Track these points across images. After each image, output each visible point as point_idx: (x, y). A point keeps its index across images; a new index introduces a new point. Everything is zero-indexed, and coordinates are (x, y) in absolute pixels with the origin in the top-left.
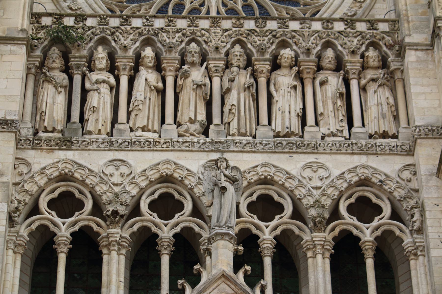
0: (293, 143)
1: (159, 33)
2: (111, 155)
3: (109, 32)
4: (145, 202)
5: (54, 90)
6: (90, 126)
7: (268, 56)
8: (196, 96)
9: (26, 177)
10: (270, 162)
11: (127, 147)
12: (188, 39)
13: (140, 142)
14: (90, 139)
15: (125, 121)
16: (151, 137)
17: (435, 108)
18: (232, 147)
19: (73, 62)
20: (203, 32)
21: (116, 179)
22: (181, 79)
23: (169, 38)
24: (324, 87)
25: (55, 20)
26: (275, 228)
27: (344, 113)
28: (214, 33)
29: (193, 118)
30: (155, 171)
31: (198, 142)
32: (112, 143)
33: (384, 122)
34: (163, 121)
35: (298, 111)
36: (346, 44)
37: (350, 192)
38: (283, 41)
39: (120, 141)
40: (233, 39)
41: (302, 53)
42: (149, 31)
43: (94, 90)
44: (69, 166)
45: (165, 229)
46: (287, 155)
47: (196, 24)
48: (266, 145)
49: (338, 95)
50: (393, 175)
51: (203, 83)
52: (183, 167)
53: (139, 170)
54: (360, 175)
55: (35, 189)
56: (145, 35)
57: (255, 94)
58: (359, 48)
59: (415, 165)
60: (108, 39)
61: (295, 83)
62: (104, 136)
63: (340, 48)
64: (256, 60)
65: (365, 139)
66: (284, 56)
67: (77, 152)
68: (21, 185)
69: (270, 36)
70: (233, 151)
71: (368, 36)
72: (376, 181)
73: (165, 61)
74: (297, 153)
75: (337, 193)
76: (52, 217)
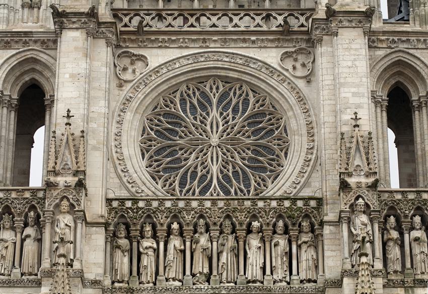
1: (181, 211)
3: (152, 211)
5: (122, 254)
6: (143, 279)
7: (244, 227)
12: (198, 215)
13: (171, 289)
14: (144, 288)
17: (338, 267)
19: (133, 233)
20: (207, 210)
22: (194, 243)
24: (276, 248)
25: (120, 204)
27: (287, 265)
28: (213, 210)
29: (201, 271)
31: (204, 288)
35: (261, 265)
38: (254, 215)
39: (160, 288)
40: (224, 215)
41: (265, 224)
42: (175, 210)
43: (145, 254)
47: (203, 204)
48: (242, 289)
58: (298, 220)
60: (151, 216)
61: (260, 245)
62: (151, 285)
64: (238, 230)
71: (304, 211)
73: (185, 232)
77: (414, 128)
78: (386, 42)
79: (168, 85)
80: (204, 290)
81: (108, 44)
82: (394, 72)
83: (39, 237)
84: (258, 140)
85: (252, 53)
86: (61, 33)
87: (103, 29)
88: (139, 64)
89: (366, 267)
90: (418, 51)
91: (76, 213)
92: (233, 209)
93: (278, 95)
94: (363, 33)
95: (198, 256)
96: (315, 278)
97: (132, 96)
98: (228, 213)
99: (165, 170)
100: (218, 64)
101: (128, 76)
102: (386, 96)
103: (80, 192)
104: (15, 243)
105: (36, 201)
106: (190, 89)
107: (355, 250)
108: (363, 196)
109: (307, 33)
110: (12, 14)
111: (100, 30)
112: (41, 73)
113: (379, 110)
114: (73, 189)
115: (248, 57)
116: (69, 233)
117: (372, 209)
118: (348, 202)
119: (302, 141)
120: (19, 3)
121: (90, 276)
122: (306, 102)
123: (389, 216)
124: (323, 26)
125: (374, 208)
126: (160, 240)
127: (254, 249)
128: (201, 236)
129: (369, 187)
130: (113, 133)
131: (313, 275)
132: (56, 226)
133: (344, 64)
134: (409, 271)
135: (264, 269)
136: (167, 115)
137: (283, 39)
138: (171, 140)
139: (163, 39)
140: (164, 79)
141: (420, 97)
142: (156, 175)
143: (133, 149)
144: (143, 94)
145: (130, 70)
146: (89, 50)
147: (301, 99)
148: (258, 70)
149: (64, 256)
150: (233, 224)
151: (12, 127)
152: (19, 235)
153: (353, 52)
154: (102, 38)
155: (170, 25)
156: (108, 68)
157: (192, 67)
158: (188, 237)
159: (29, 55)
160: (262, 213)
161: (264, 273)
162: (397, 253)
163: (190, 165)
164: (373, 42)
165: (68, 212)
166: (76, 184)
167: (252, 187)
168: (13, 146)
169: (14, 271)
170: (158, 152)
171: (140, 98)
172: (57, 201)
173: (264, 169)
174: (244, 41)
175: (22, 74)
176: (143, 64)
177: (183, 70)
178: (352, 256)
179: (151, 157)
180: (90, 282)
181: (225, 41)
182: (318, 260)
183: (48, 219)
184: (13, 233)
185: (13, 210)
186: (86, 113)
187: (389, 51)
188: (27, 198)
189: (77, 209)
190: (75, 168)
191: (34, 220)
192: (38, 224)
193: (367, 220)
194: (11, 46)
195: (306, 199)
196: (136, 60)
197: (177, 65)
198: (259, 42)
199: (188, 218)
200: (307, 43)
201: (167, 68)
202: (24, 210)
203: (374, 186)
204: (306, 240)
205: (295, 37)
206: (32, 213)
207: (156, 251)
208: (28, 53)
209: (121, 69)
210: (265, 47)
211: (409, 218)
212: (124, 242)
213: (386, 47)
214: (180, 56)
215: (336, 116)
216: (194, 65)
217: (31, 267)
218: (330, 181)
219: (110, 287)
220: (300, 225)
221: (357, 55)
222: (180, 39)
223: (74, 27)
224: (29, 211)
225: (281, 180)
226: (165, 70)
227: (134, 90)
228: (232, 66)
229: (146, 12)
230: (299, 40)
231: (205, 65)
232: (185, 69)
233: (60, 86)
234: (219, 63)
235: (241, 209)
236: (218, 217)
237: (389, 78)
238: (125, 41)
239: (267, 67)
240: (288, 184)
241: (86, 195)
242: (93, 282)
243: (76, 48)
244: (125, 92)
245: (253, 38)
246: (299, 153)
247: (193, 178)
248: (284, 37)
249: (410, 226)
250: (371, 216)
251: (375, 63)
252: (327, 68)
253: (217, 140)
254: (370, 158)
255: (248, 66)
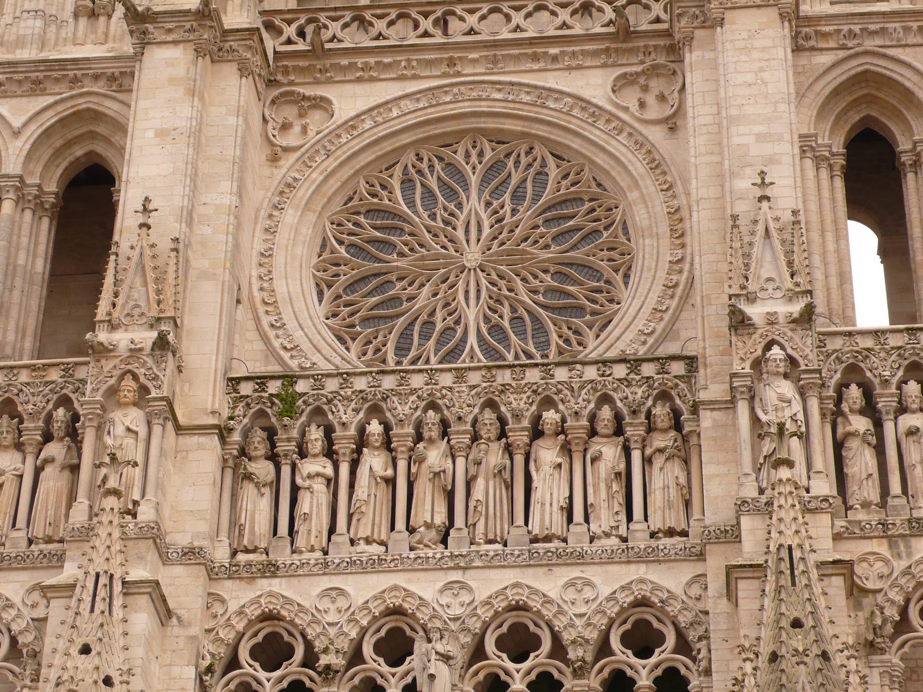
0: (552, 552)
2: (327, 582)
4: (368, 642)
5: (256, 491)
6: (300, 542)
7: (526, 423)
8: (434, 486)
9: (222, 621)
10: (523, 581)
11: (346, 568)
14: (300, 561)
15: (345, 530)
16: (375, 553)
18: (477, 560)
21: (330, 618)
22: (415, 463)
23: (400, 404)
24: (596, 465)
26: (528, 673)
27: (621, 501)
28: (459, 392)
29: (429, 521)
30: (380, 601)
31: (434, 557)
32: (326, 565)
33: (670, 514)
34: (393, 528)
36: (626, 398)
37: (624, 616)
39: (337, 561)
40: (482, 400)
44: (274, 600)
45: (393, 681)
46: (546, 569)
48: (519, 556)
49: (613, 476)
50: (678, 591)
51: (442, 468)
52: (414, 594)
53: (361, 601)
54: (636, 593)
55: (231, 636)
56: (371, 400)
57: (509, 480)
58: (644, 404)
59: (705, 575)
61: (559, 460)
62: (318, 554)
63: (619, 404)
65: (646, 540)
66: (547, 421)
67: (284, 580)
68: (214, 632)
69: (529, 393)
70: (478, 567)
71: (656, 384)
72: (657, 601)
73: (395, 439)
74: (558, 565)
75: (605, 621)
76: (254, 672)
77: (906, 209)
78: (835, 37)
79: (375, 152)
80: (435, 561)
81: (244, 70)
82: (855, 96)
83: (75, 461)
84: (567, 251)
85: (553, 80)
86: (143, 54)
87: (232, 43)
88: (315, 119)
89: (789, 488)
90: (908, 50)
91: (151, 404)
92: (500, 388)
93: (608, 159)
94: (778, 16)
95: (424, 489)
96: (683, 526)
97: (298, 176)
98: (491, 396)
99: (366, 320)
100: (480, 106)
101: (291, 139)
102: (841, 146)
103: (163, 361)
104: (21, 477)
105: (71, 387)
106: (422, 159)
107: (765, 457)
108: (782, 341)
109: (668, 34)
110: (53, 28)
111: (227, 45)
112: (107, 140)
113: (824, 174)
114: (147, 356)
115: (544, 88)
116: (133, 447)
117: (803, 367)
118: (748, 355)
119: (658, 249)
120: (70, 7)
121: (180, 538)
122: (666, 169)
123: (847, 386)
124: (693, 9)
125: (807, 365)
126: (341, 459)
127: (547, 469)
128: (431, 447)
129: (794, 321)
130: (254, 251)
131: (678, 520)
132: (106, 433)
133: (740, 78)
134: (897, 501)
135: (569, 511)
136: (371, 212)
137: (617, 50)
138: (380, 261)
139: (366, 63)
140: (368, 141)
141: (915, 144)
142: (346, 332)
143: (298, 282)
144: (321, 173)
145: (297, 129)
146: (198, 82)
147: (656, 166)
148: (564, 113)
149: (116, 493)
150: (502, 421)
151: (42, 248)
152: (30, 460)
153: (756, 55)
154: (230, 61)
155: (379, 36)
156: (240, 118)
157: (426, 115)
158: (403, 449)
159: (82, 103)
160: (566, 392)
161: (570, 520)
162: (867, 464)
163: (420, 308)
164: (807, 38)
165: (135, 404)
166: (154, 343)
167: (553, 348)
168: (42, 287)
169: (15, 534)
170: (351, 287)
171: (315, 180)
172: (112, 381)
173: (579, 310)
174: (535, 58)
175: (69, 144)
176: (325, 115)
177: (406, 121)
178: (760, 469)
179: (339, 297)
180: (179, 550)
181: (495, 60)
182: (690, 488)
183: (90, 419)
184: (18, 456)
185: (20, 408)
186: (186, 203)
187: (842, 54)
188: (53, 382)
189: (153, 395)
190: (154, 313)
191: (64, 425)
192: (73, 435)
193: (792, 392)
194: (45, 89)
195: (662, 359)
196: (309, 107)
197: (395, 112)
198: (566, 58)
199: (403, 410)
200: (668, 54)
201: (373, 118)
202: (44, 407)
203: (807, 317)
204: (662, 445)
205: (641, 44)
206: (61, 411)
207: (332, 483)
208: (80, 101)
209: (278, 127)
210: (579, 68)
211: (894, 386)
212: (263, 469)
213: (836, 46)
214: (401, 93)
215: (723, 186)
216: (429, 110)
217: (50, 524)
218: (712, 318)
219: (226, 562)
220: (649, 415)
221: (767, 60)
222: (401, 61)
223: (169, 39)
224: (56, 407)
225: (614, 330)
226: (368, 124)
227: (302, 166)
228: (511, 109)
229: (333, 14)
230: (652, 49)
231: (452, 109)
232: (411, 120)
233: (134, 154)
234: (483, 103)
235: (518, 386)
236: (469, 406)
237: (846, 111)
238: (286, 71)
239: (584, 105)
240: (630, 335)
241: (180, 369)
242: (186, 550)
243: (172, 81)
244: (284, 170)
245: (554, 51)
246: (653, 271)
247: (425, 336)
248: (619, 45)
249: (895, 404)
250: (802, 383)
251: (811, 80)
252: (703, 92)
253: (477, 256)
254: (796, 262)
255: (543, 106)
